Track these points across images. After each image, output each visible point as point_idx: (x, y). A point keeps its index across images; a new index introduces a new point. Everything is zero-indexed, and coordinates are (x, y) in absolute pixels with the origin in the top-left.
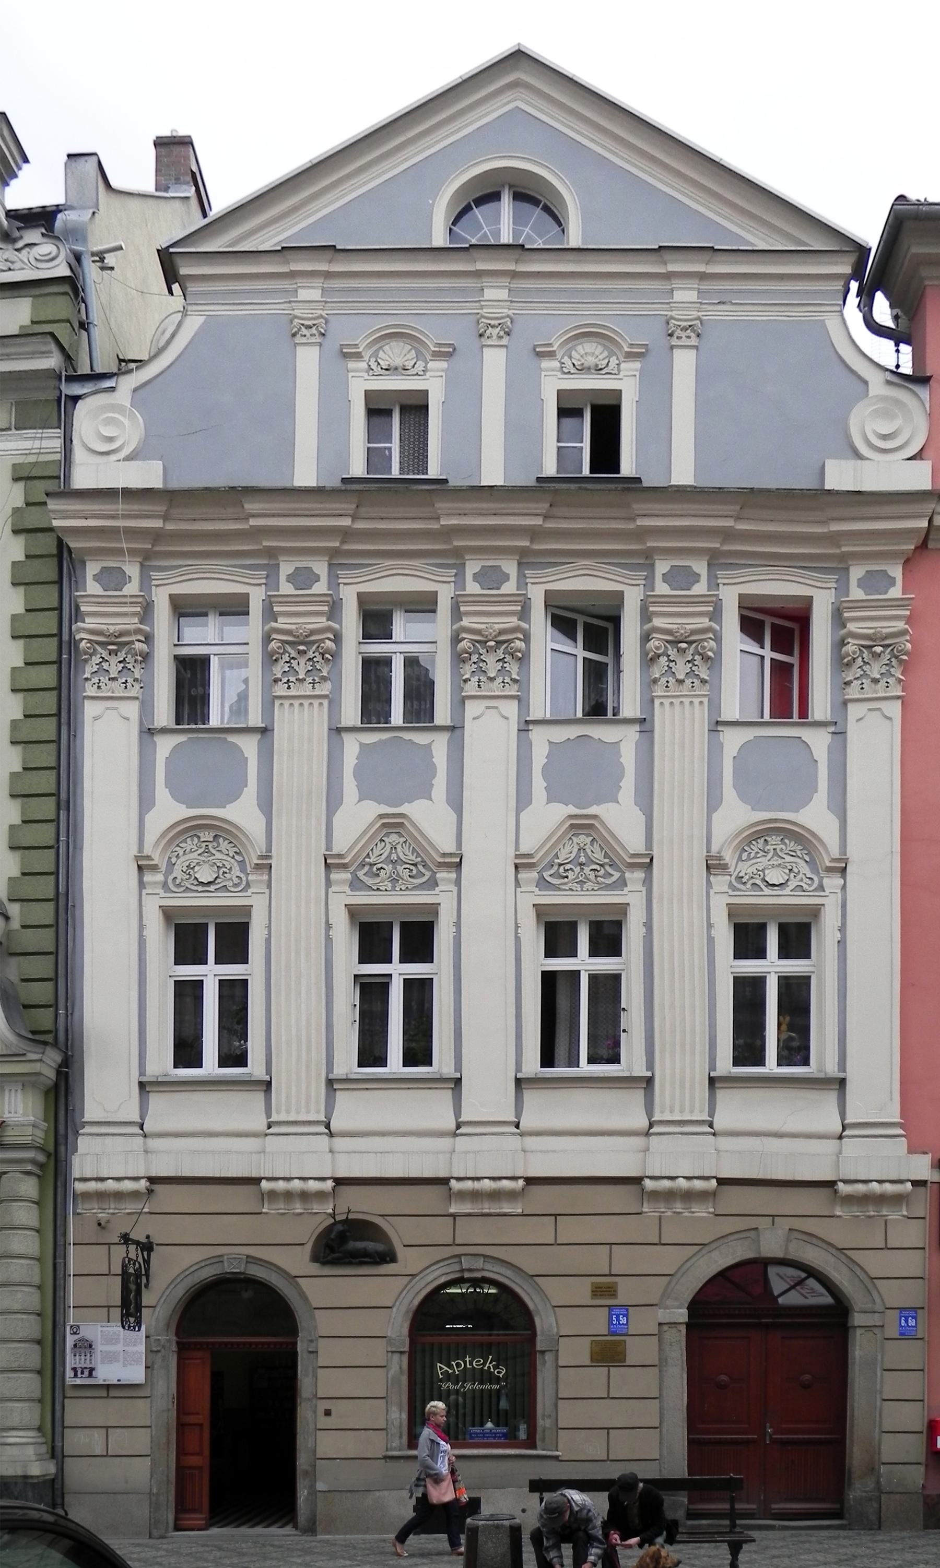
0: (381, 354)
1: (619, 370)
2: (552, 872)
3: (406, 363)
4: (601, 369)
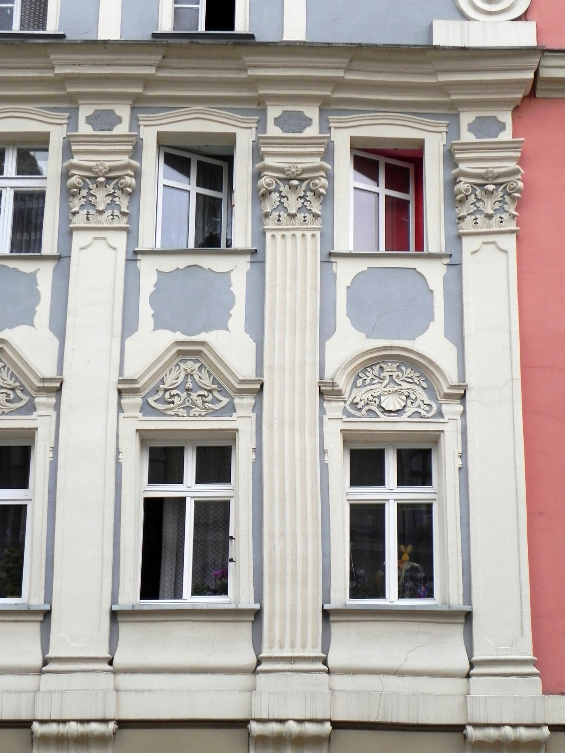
2: (157, 397)
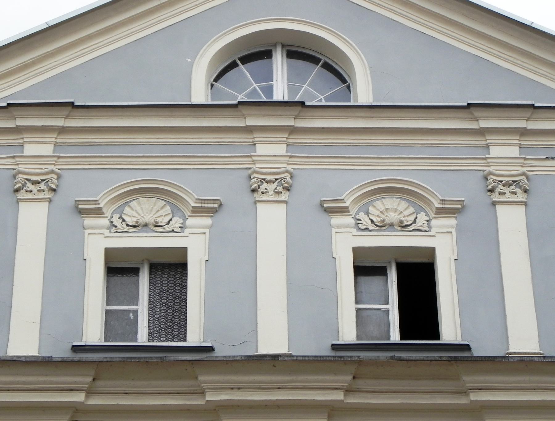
0: (127, 210)
1: (430, 227)
3: (159, 220)
4: (407, 226)
